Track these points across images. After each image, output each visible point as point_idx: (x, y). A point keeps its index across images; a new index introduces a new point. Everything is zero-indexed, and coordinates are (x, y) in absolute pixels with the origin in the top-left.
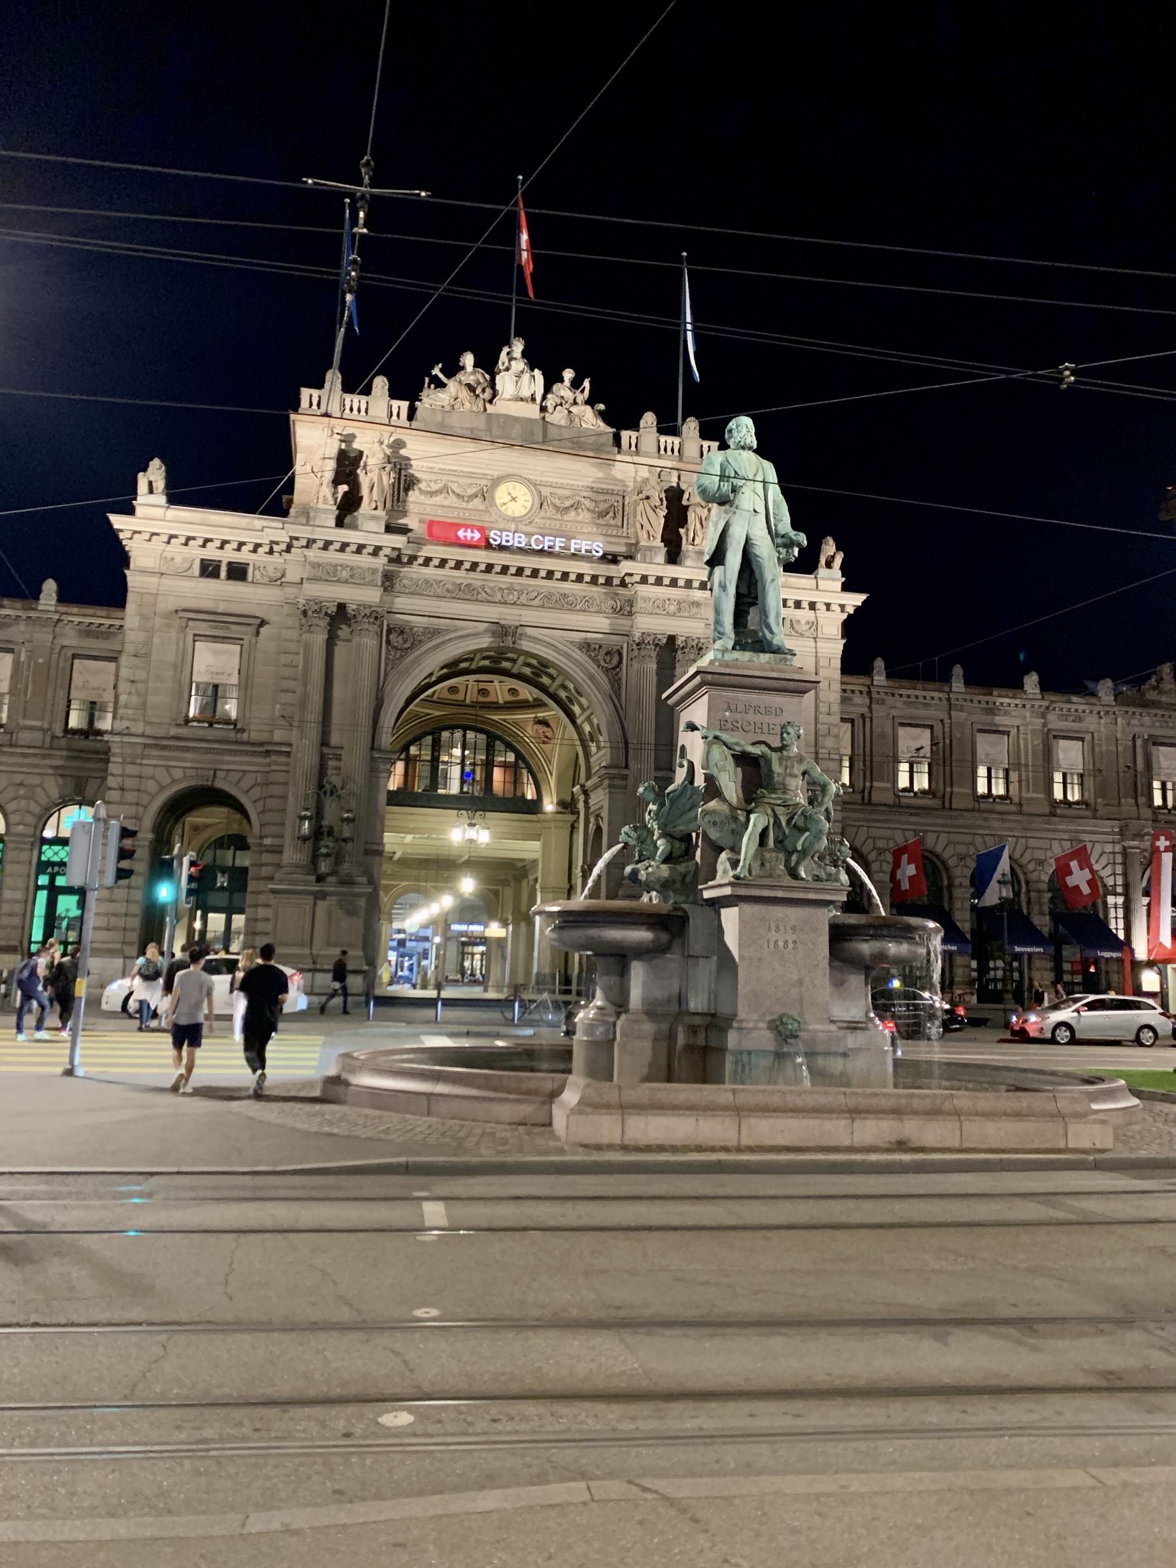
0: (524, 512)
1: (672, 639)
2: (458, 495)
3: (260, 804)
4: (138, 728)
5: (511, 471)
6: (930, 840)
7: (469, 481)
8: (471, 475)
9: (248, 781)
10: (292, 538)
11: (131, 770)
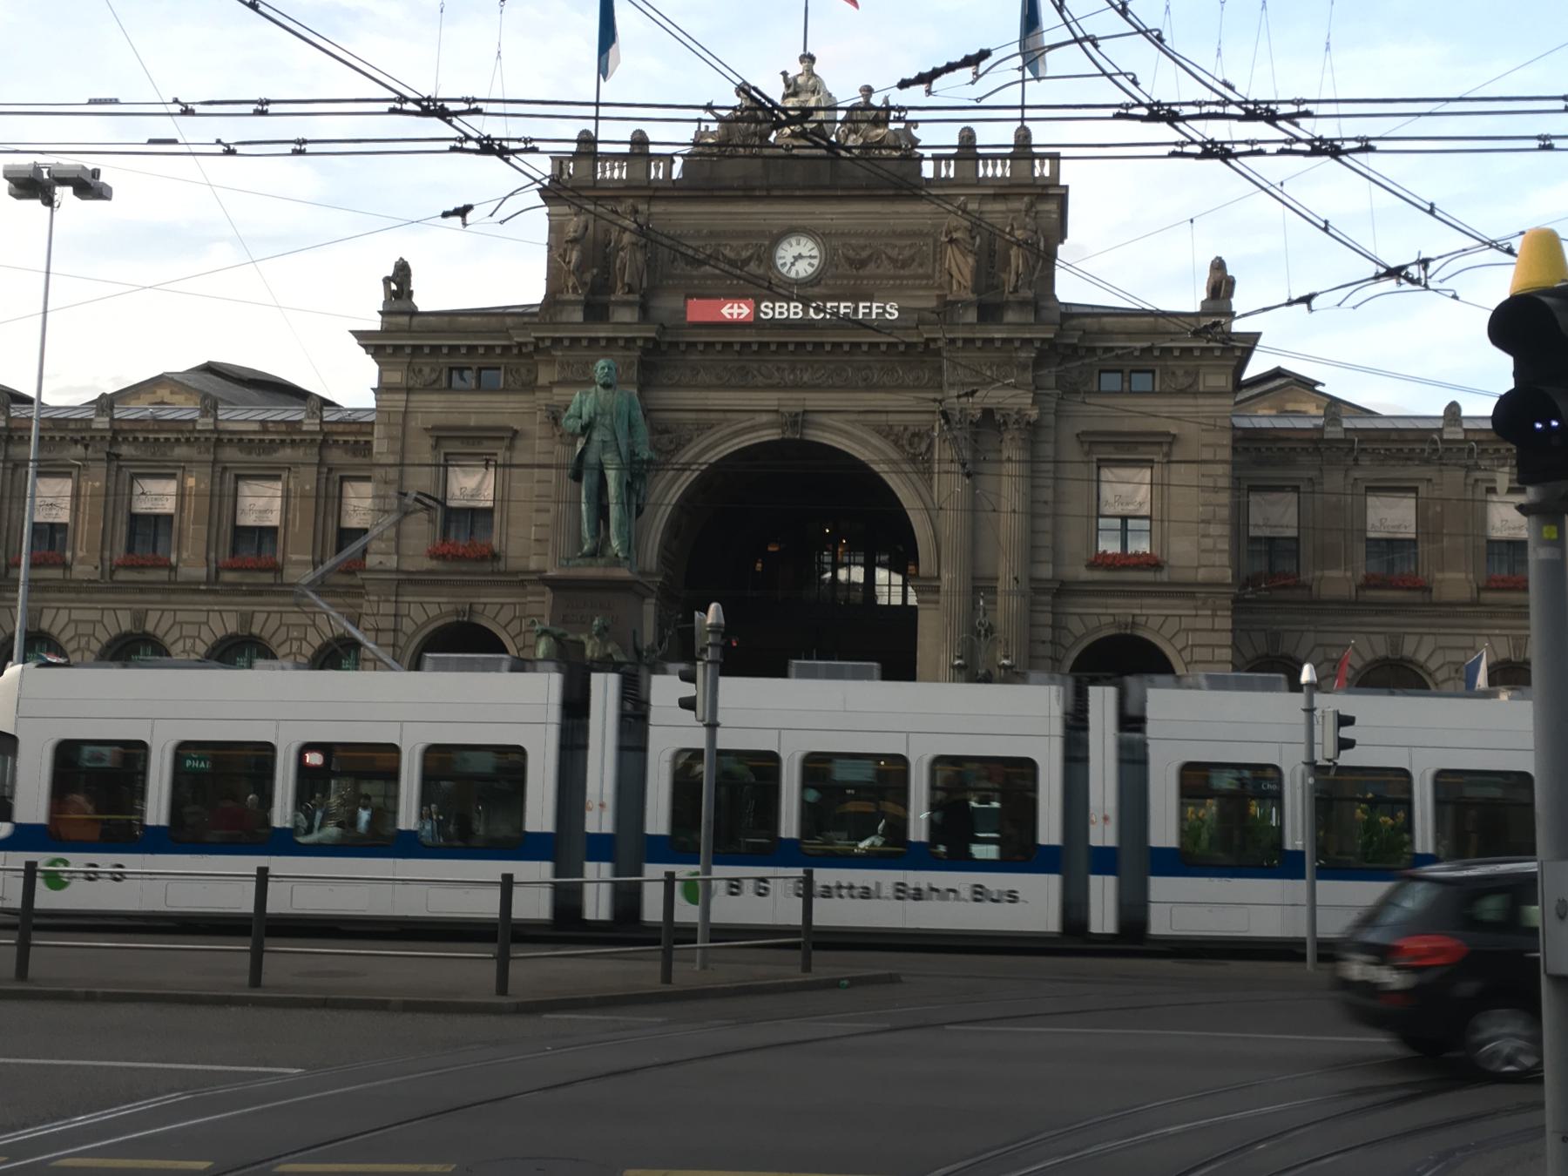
0: (810, 270)
1: (988, 413)
2: (732, 263)
3: (520, 640)
4: (392, 562)
5: (794, 222)
6: (1408, 649)
7: (742, 243)
8: (745, 234)
9: (505, 616)
10: (537, 338)
11: (388, 608)
